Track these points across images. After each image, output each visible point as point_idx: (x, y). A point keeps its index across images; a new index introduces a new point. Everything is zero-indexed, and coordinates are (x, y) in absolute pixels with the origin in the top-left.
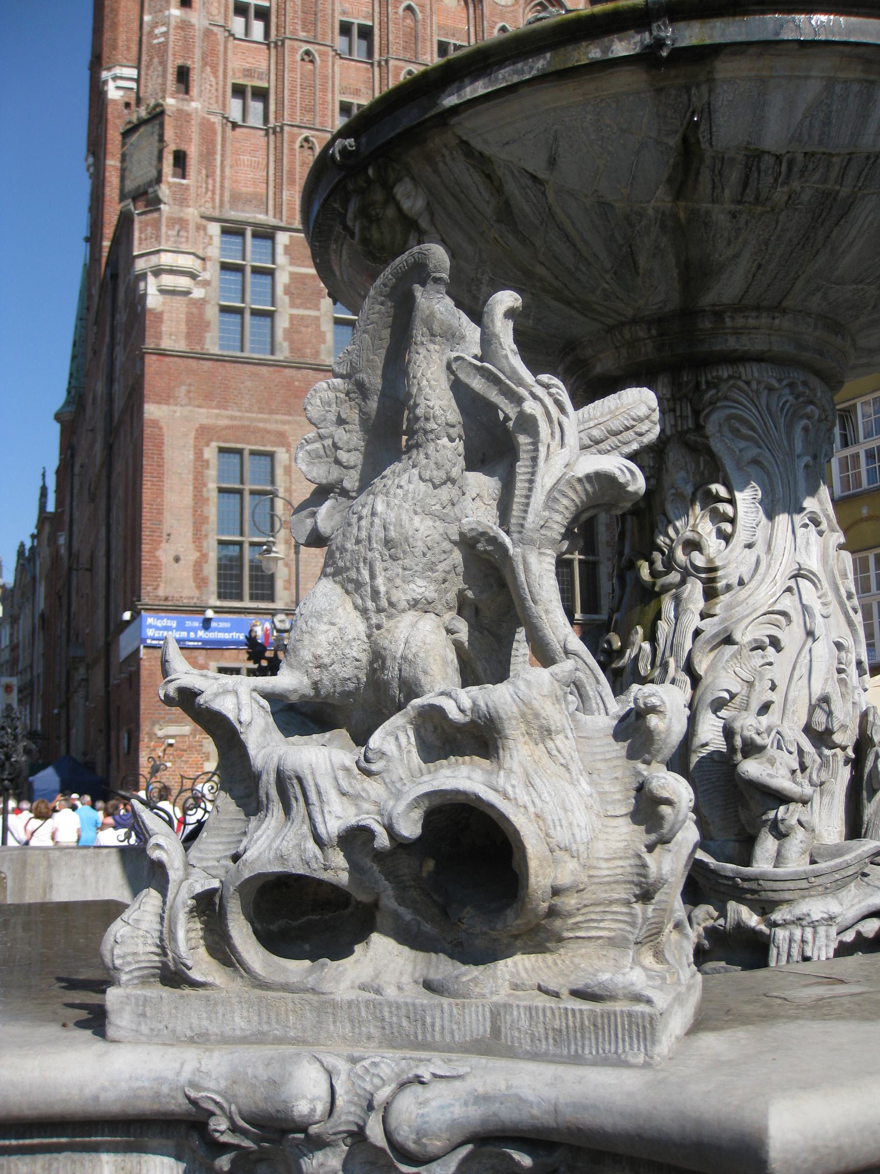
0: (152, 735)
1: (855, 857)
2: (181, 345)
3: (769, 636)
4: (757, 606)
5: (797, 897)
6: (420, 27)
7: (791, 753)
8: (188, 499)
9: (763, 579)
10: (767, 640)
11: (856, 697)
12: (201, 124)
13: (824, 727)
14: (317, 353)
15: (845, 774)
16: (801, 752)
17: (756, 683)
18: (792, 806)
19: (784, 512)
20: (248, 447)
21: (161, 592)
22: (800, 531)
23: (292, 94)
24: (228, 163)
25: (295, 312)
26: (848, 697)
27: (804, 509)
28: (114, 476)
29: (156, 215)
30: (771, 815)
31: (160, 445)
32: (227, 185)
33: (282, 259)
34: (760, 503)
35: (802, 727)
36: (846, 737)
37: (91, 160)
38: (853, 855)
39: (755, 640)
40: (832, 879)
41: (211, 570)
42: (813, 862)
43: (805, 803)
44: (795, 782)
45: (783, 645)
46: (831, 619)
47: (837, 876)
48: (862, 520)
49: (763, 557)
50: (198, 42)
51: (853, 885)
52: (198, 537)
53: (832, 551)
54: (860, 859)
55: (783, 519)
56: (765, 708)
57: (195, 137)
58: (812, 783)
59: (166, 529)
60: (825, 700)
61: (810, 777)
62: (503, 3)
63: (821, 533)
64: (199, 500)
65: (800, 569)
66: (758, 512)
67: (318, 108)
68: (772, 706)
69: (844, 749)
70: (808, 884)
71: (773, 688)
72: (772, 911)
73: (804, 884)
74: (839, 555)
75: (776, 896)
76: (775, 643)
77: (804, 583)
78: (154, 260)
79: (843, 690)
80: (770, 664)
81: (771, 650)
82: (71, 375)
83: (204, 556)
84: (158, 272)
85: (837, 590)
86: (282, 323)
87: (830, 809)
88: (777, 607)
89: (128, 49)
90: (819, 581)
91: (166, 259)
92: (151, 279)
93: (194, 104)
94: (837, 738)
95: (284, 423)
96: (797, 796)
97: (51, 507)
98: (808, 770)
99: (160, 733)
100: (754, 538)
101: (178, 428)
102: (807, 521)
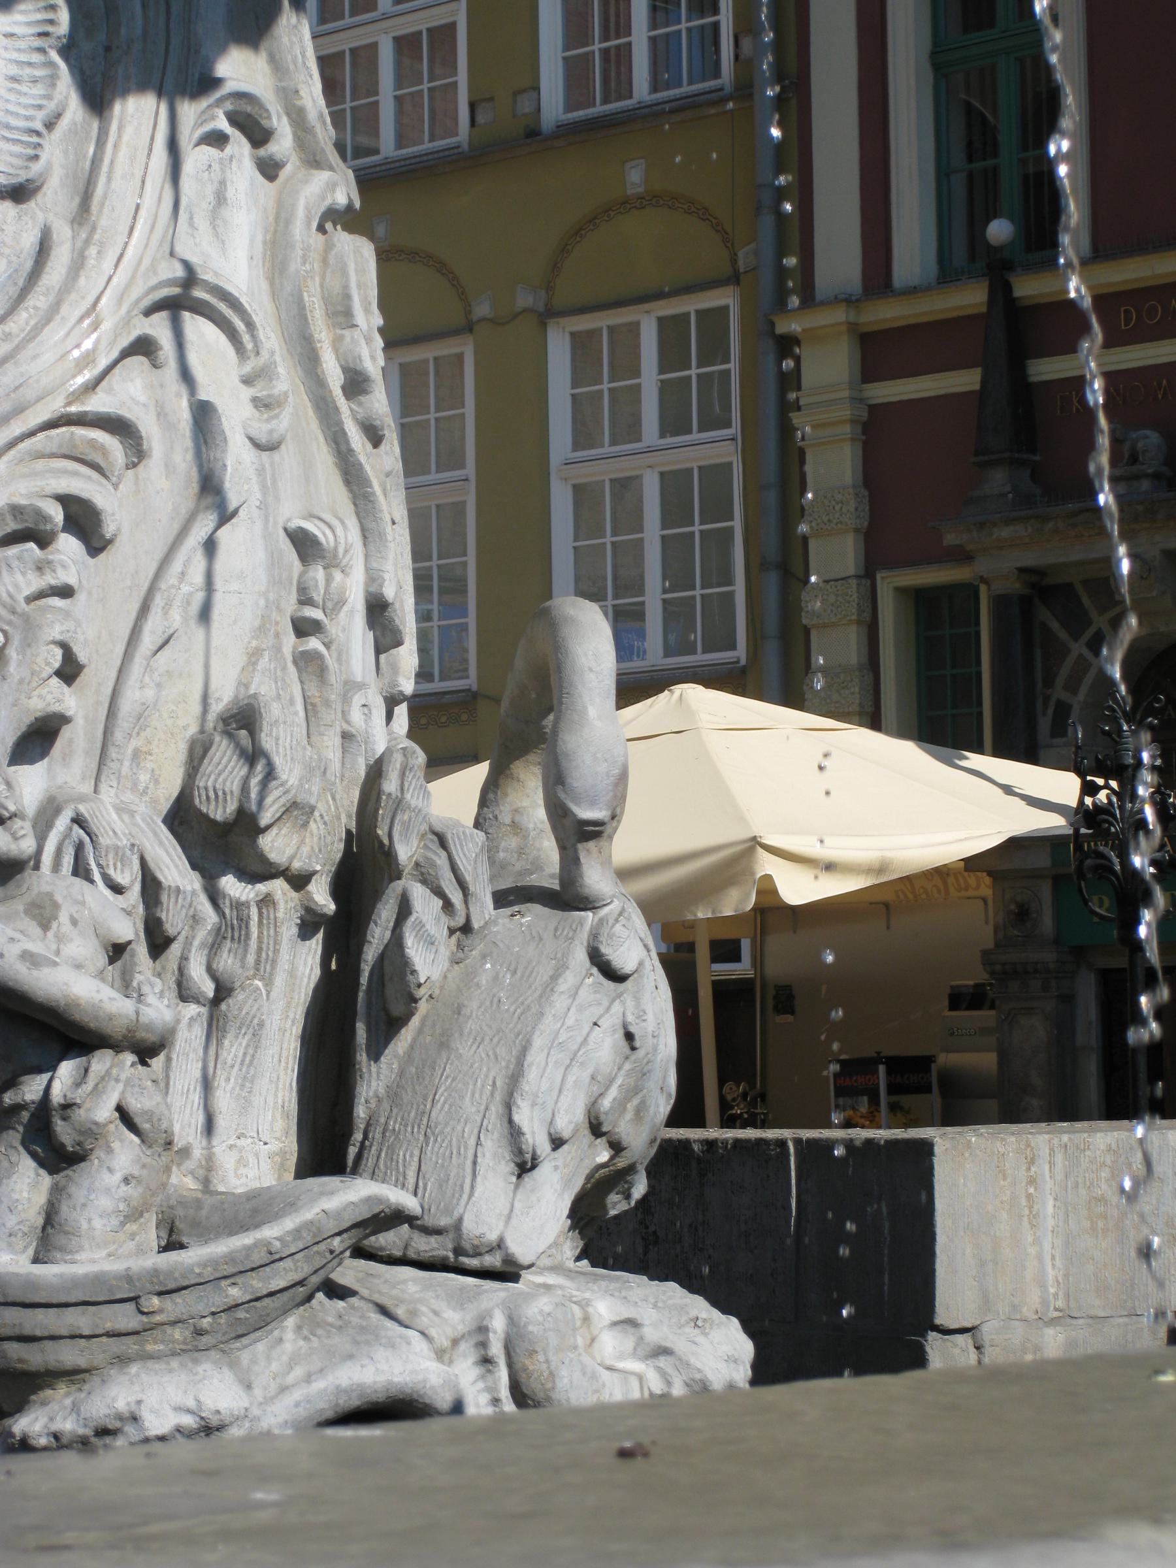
1: (297, 1232)
3: (65, 500)
4: (29, 394)
5: (99, 1358)
7: (117, 889)
9: (55, 308)
10: (57, 514)
11: (356, 716)
13: (232, 807)
15: (302, 964)
16: (151, 887)
17: (12, 653)
18: (101, 1061)
19: (142, 87)
22: (196, 158)
26: (327, 716)
27: (217, 83)
30: (31, 1089)
34: (68, 50)
35: (165, 806)
36: (307, 845)
38: (289, 1223)
39: (16, 510)
40: (218, 1301)
42: (172, 1244)
43: (146, 1050)
44: (126, 986)
45: (109, 529)
46: (287, 456)
47: (235, 1293)
48: (626, 204)
49: (63, 233)
51: (291, 1321)
53: (302, 231)
54: (313, 1239)
55: (138, 114)
56: (38, 738)
58: (184, 993)
60: (243, 721)
61: (181, 970)
63: (269, 169)
65: (190, 278)
66: (53, 79)
68: (66, 733)
69: (299, 881)
70: (138, 1318)
71: (69, 671)
72: (19, 1407)
73: (124, 1318)
74: (329, 247)
75: (34, 1357)
76: (83, 520)
77: (198, 328)
79: (313, 691)
80: (65, 592)
81: (68, 545)
85: (309, 359)
87: (247, 1081)
88: (98, 404)
90: (250, 325)
94: (277, 845)
96: (116, 1029)
98: (175, 949)
100: (36, 168)
102: (223, 124)
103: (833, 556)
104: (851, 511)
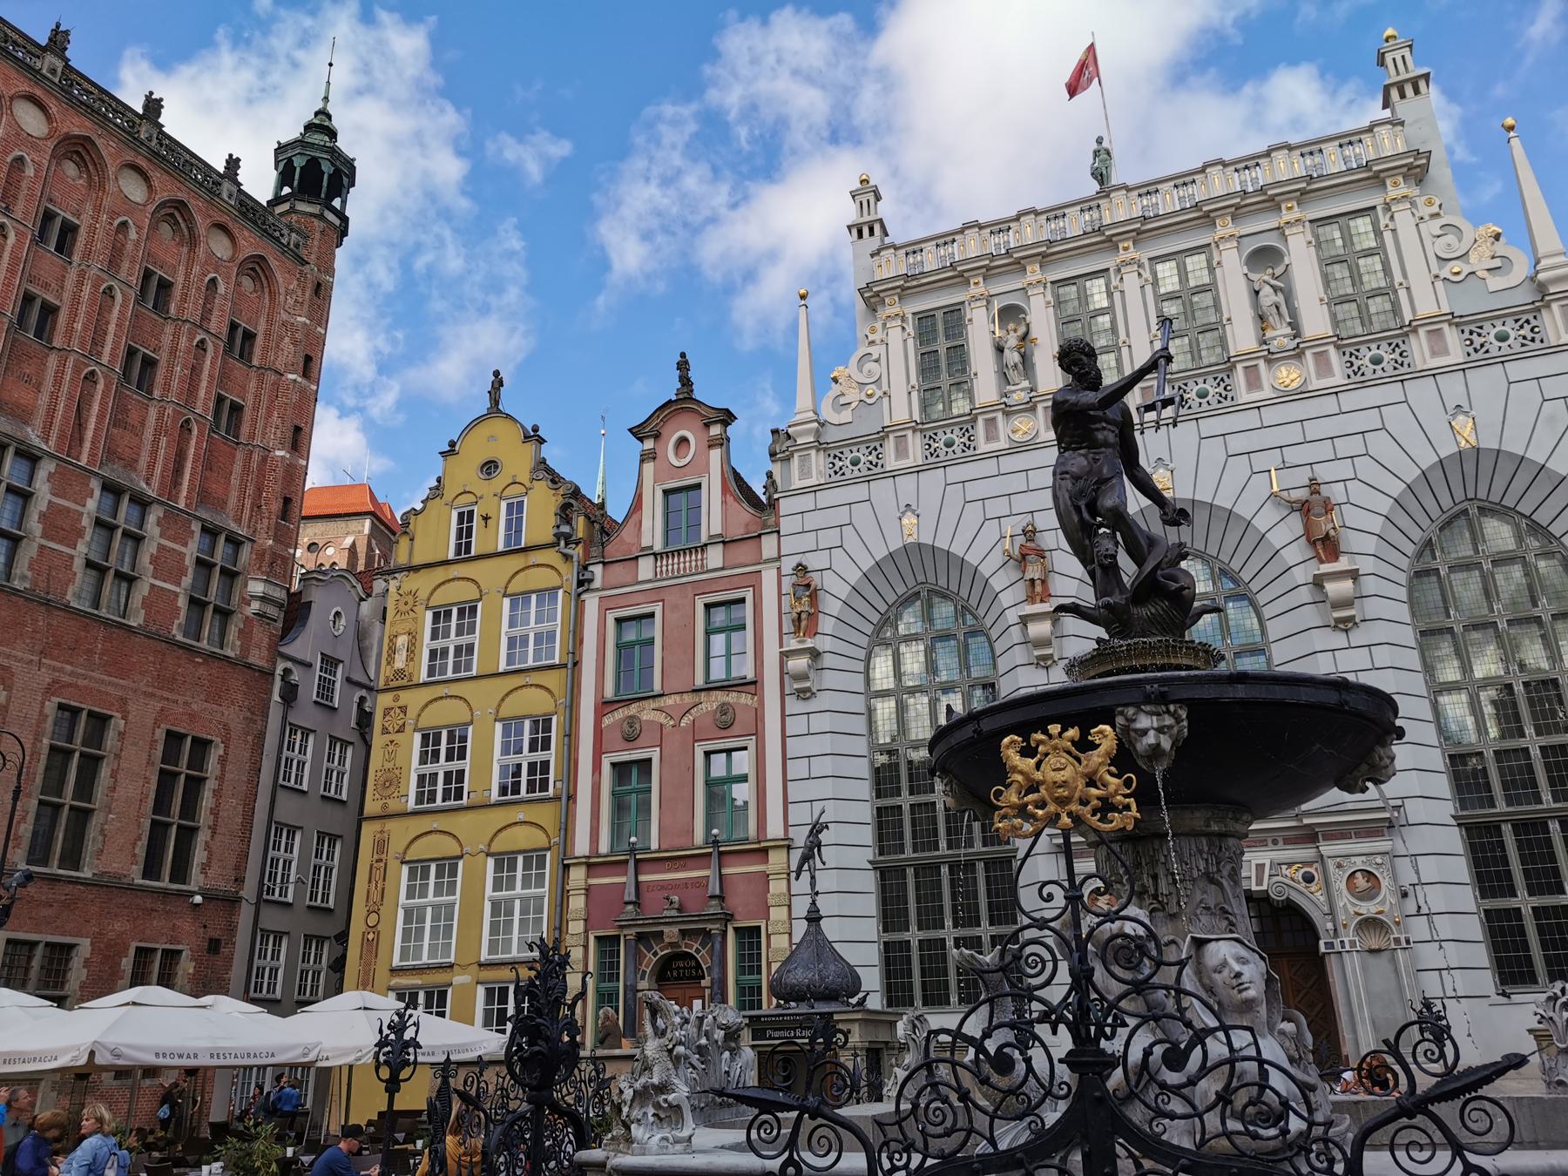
6: (130, 246)
103: (576, 927)
104: (583, 915)
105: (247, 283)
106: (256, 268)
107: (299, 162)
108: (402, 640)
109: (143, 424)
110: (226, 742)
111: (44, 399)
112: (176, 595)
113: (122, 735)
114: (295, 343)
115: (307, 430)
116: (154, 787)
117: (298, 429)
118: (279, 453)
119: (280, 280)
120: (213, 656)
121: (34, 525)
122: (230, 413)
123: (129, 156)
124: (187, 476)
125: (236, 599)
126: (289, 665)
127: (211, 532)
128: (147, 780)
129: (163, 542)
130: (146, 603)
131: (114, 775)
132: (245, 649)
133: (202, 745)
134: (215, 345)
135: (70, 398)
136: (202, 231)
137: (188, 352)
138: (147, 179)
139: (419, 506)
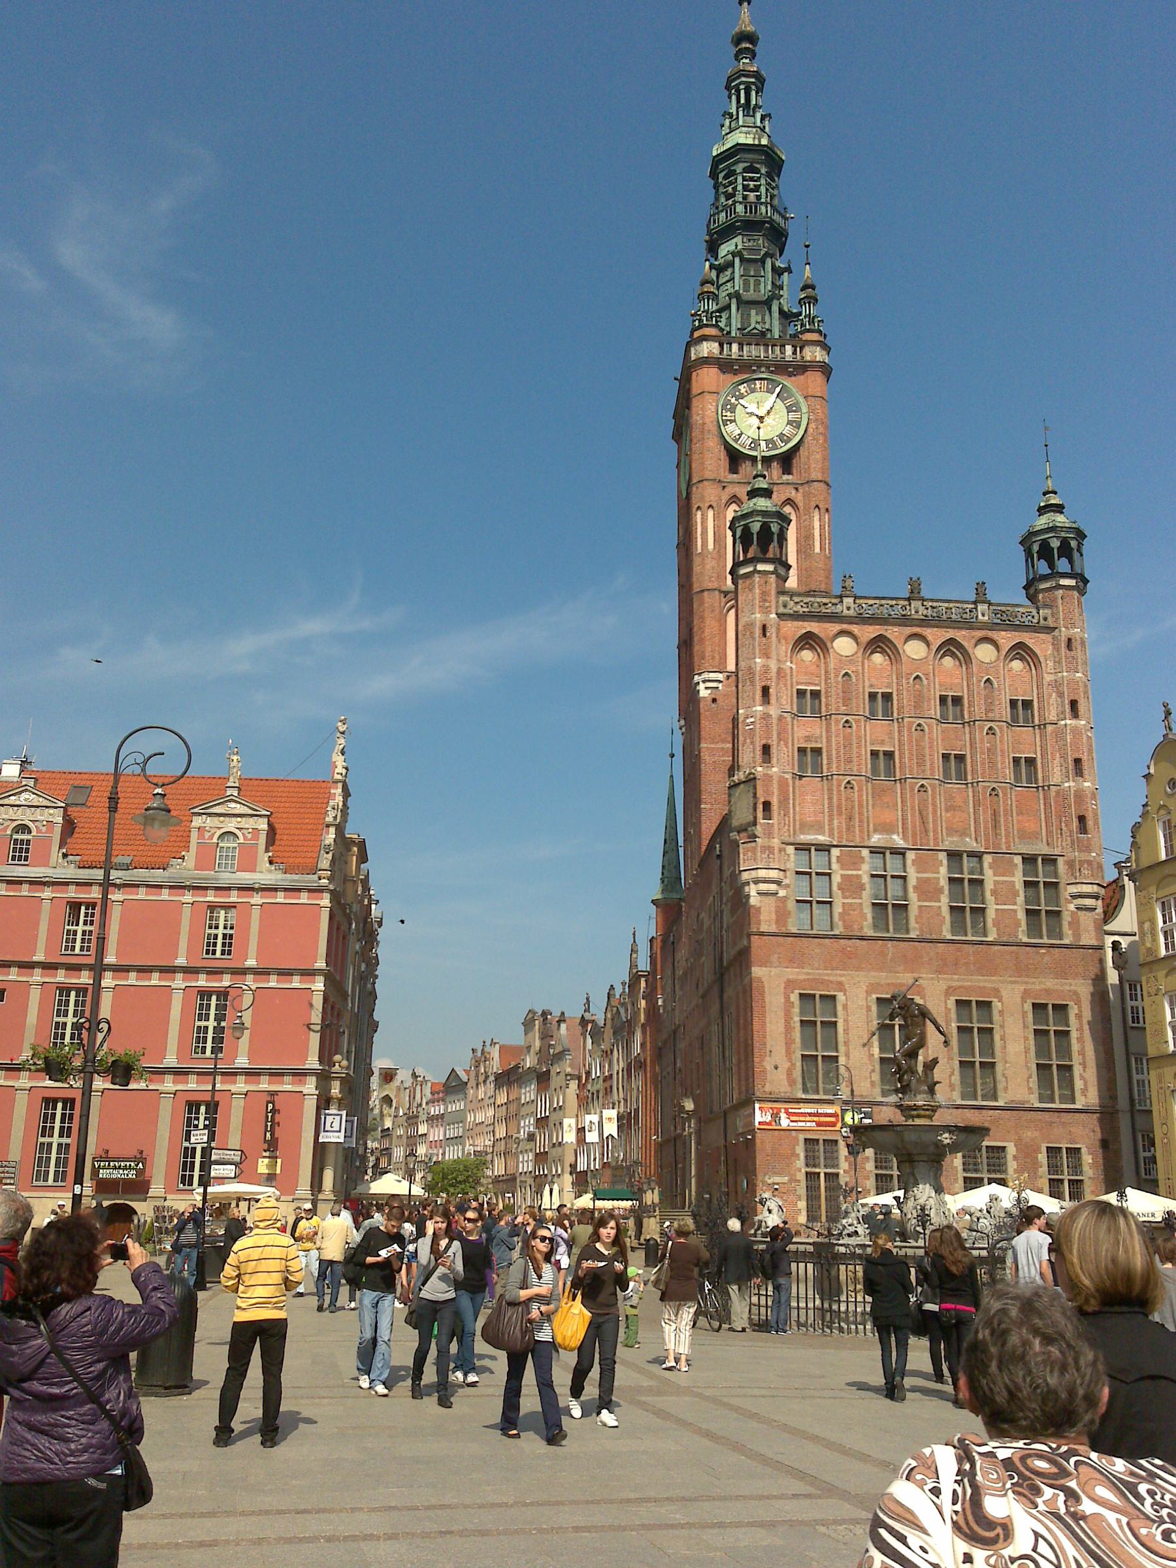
0: (763, 1182)
2: (773, 929)
6: (925, 691)
8: (782, 1029)
12: (779, 781)
14: (862, 928)
20: (818, 993)
21: (768, 1088)
23: (838, 753)
24: (797, 803)
25: (846, 901)
28: (725, 996)
29: (753, 844)
31: (762, 993)
32: (797, 818)
33: (835, 866)
37: (682, 722)
41: (797, 1074)
50: (775, 728)
52: (789, 1053)
57: (776, 791)
59: (768, 1048)
62: (987, 661)
64: (788, 1028)
67: (855, 760)
78: (754, 874)
82: (663, 867)
83: (793, 1065)
84: (757, 881)
86: (838, 909)
89: (713, 658)
91: (762, 874)
92: (752, 886)
93: (775, 769)
95: (841, 976)
97: (644, 964)
99: (769, 1181)
101: (774, 982)
105: (1017, 665)
106: (1021, 651)
107: (1036, 547)
108: (1147, 925)
109: (966, 802)
110: (1078, 1003)
111: (900, 813)
112: (1015, 911)
113: (1001, 1012)
114: (1061, 695)
115: (1085, 758)
116: (1032, 1042)
117: (1078, 761)
118: (1067, 785)
119: (1038, 652)
120: (1052, 946)
121: (912, 895)
122: (1027, 766)
123: (909, 630)
124: (1003, 828)
125: (1062, 901)
126: (1117, 938)
127: (1029, 860)
128: (1026, 1039)
129: (997, 878)
130: (996, 923)
131: (1003, 1038)
132: (1077, 935)
133: (1061, 1009)
134: (1001, 728)
135: (913, 808)
136: (970, 651)
137: (982, 741)
138: (922, 638)
139: (1140, 820)
